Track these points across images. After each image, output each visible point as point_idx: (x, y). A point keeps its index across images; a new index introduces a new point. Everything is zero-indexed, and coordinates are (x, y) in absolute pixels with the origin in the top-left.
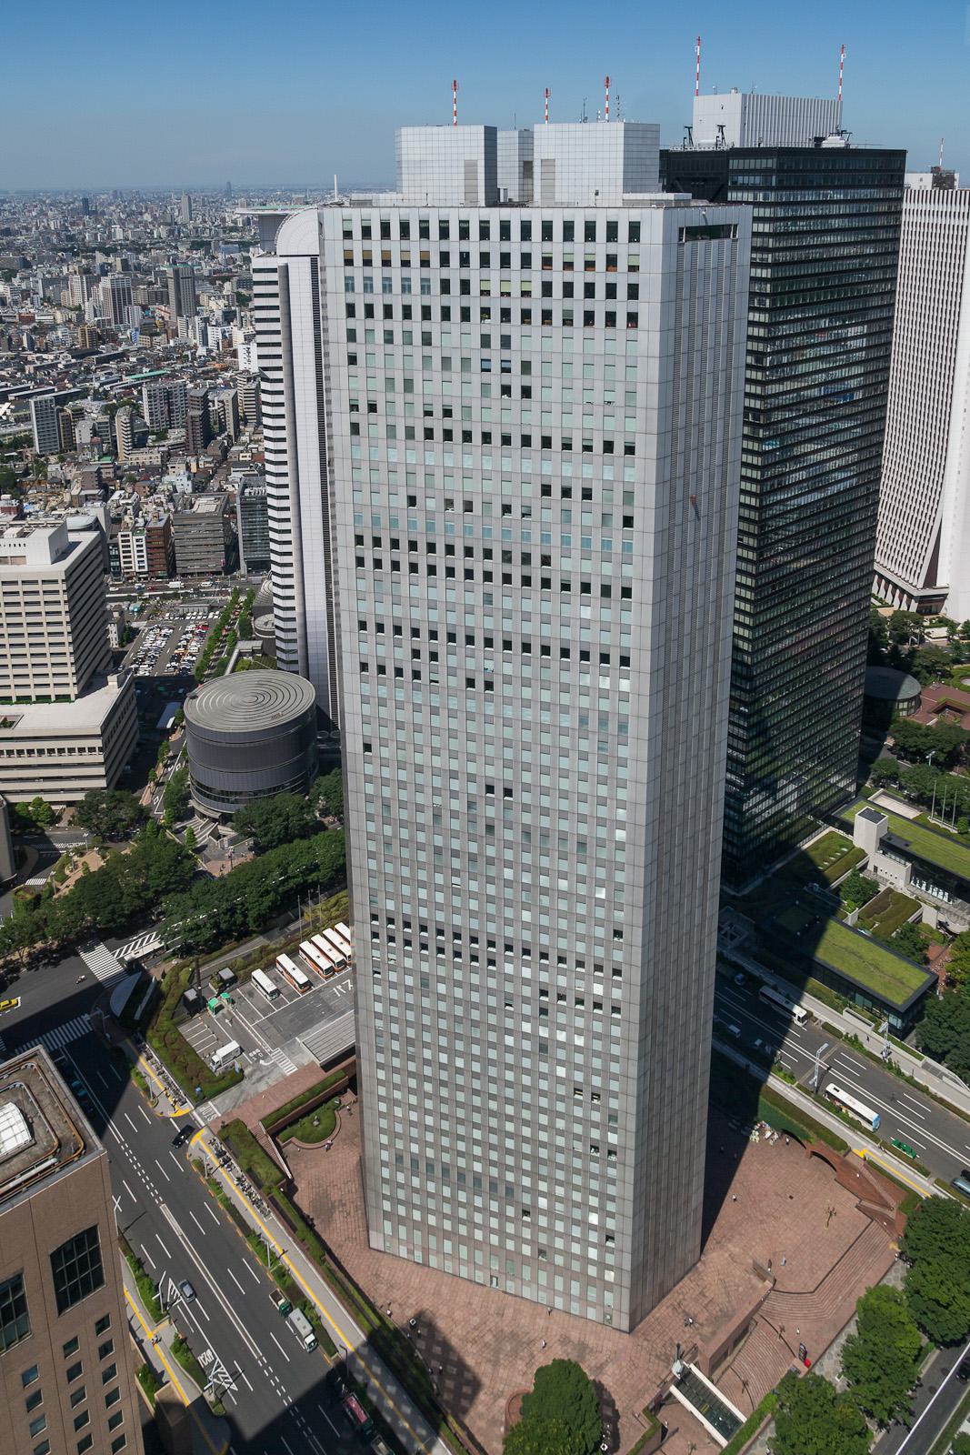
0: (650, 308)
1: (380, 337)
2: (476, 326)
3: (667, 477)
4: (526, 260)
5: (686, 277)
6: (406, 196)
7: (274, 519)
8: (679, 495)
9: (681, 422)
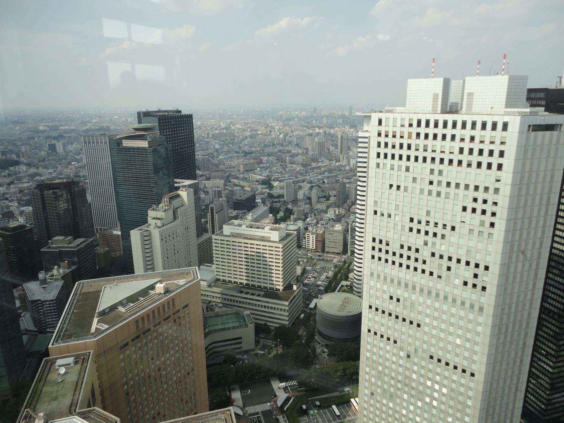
0: (509, 162)
1: (389, 167)
2: (429, 165)
3: (510, 240)
4: (453, 137)
5: (530, 149)
6: (407, 108)
7: (357, 236)
8: (515, 249)
9: (520, 215)
